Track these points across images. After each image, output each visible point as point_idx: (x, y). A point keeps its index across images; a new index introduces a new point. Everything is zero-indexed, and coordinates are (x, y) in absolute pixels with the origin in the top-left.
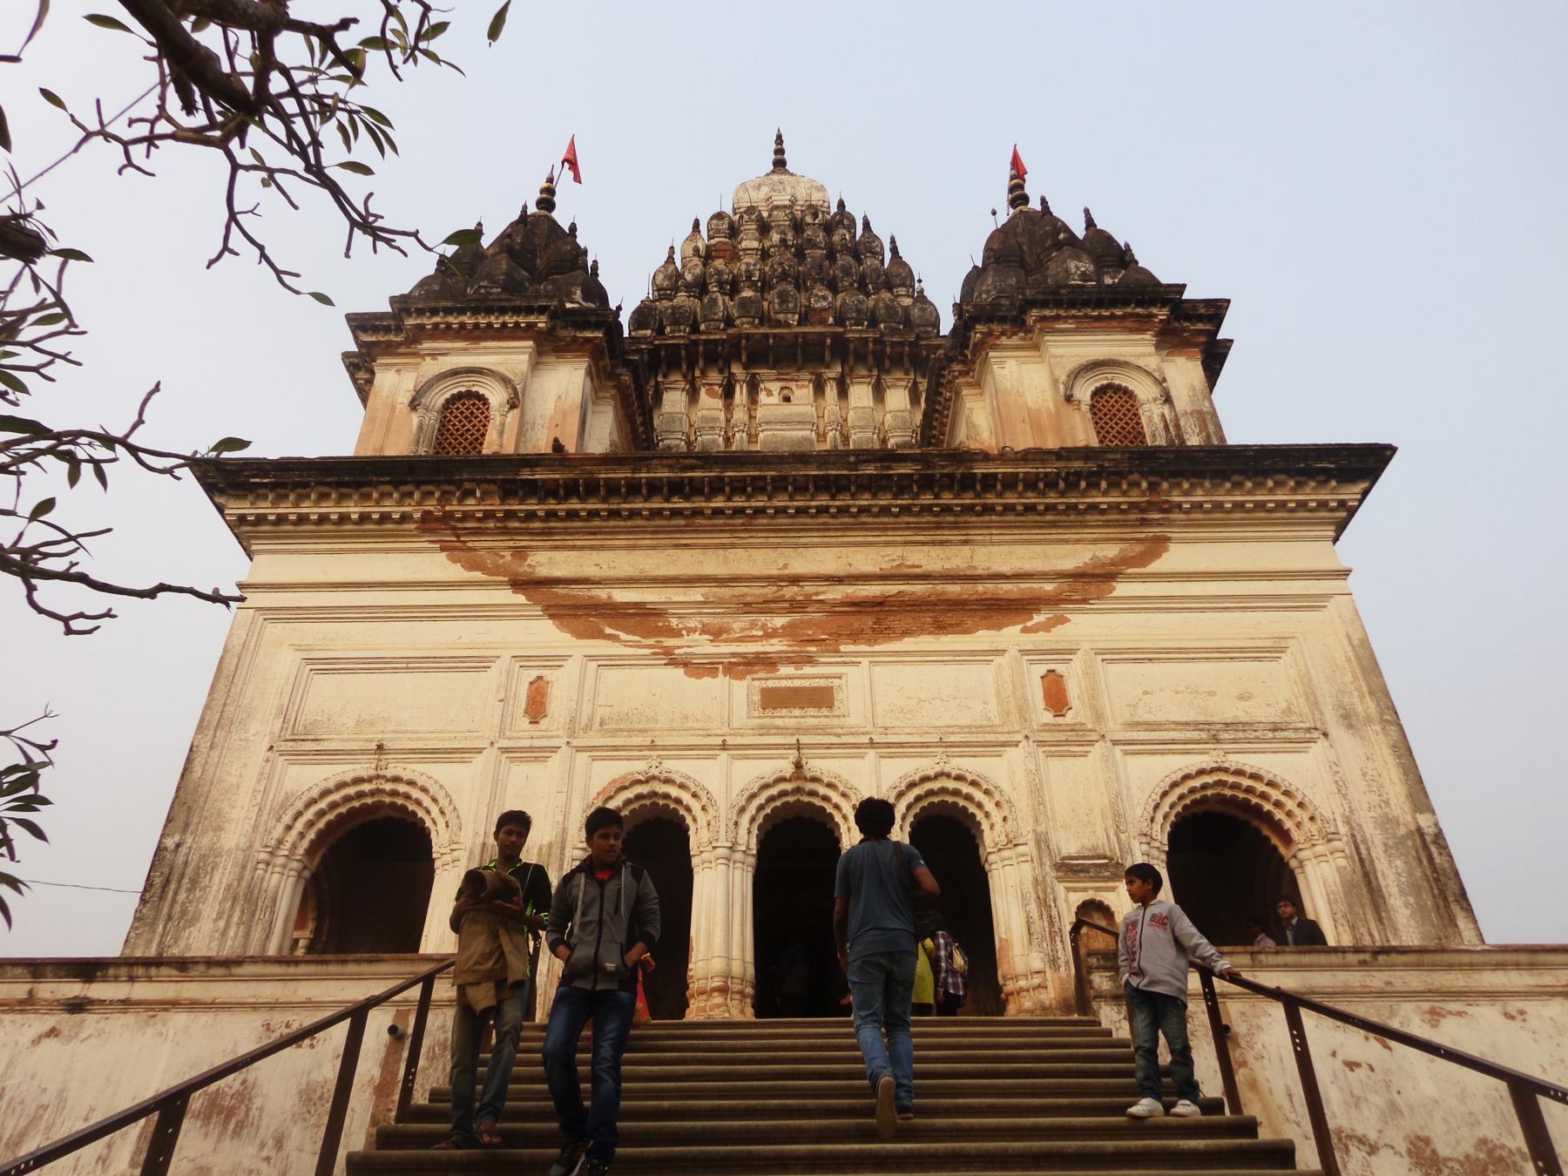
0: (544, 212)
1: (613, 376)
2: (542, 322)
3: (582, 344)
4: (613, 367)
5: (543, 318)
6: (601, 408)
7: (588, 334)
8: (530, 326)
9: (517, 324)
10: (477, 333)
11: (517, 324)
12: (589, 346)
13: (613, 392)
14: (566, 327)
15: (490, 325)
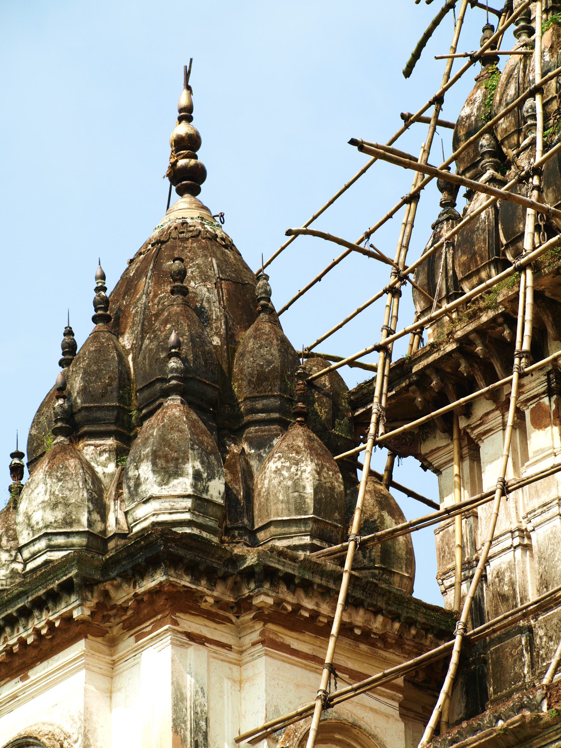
0: (183, 207)
1: (242, 605)
2: (77, 608)
3: (152, 602)
4: (236, 589)
5: (74, 600)
6: (249, 671)
7: (149, 584)
8: (67, 619)
9: (50, 624)
10: (17, 662)
11: (50, 624)
12: (161, 601)
13: (259, 626)
14: (118, 587)
15: (22, 642)
